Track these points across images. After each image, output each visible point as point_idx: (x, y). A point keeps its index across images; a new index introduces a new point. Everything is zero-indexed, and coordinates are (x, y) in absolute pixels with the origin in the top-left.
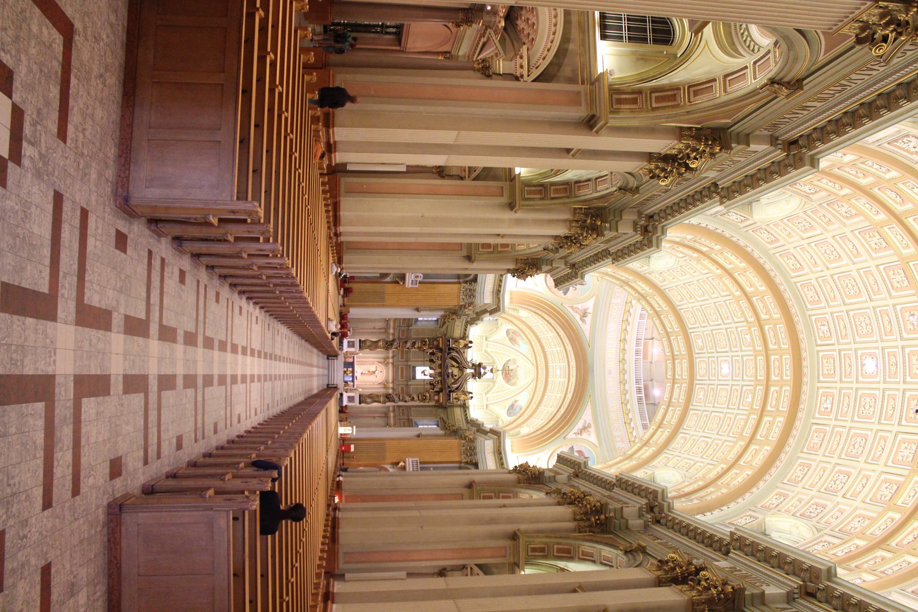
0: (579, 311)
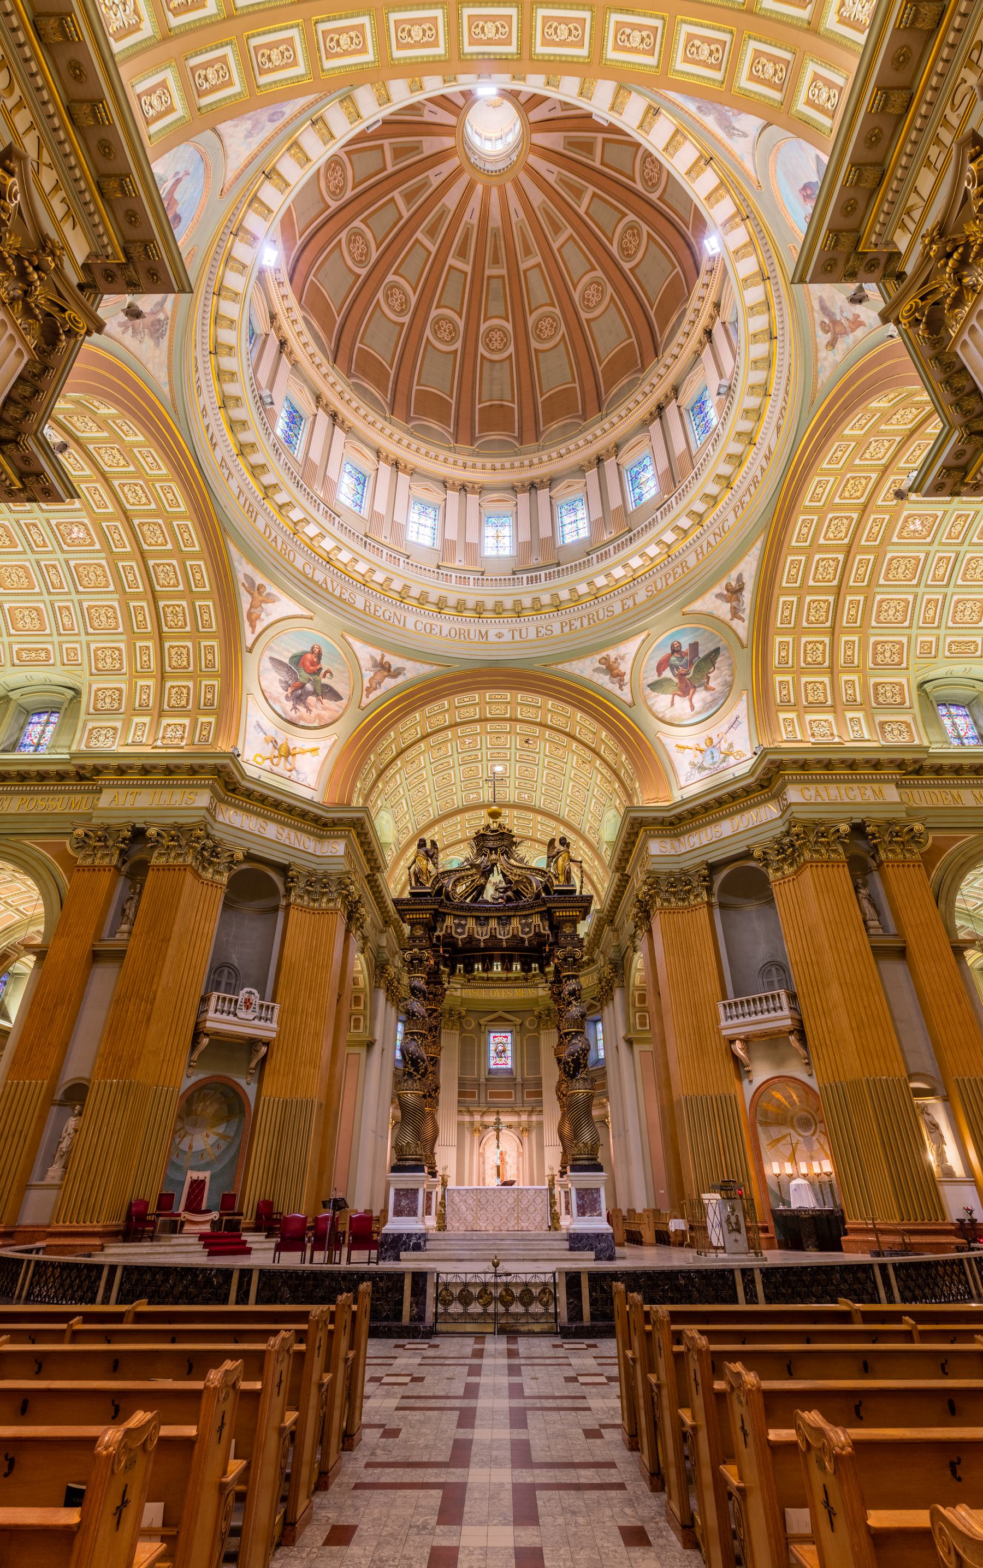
0: (378, 677)
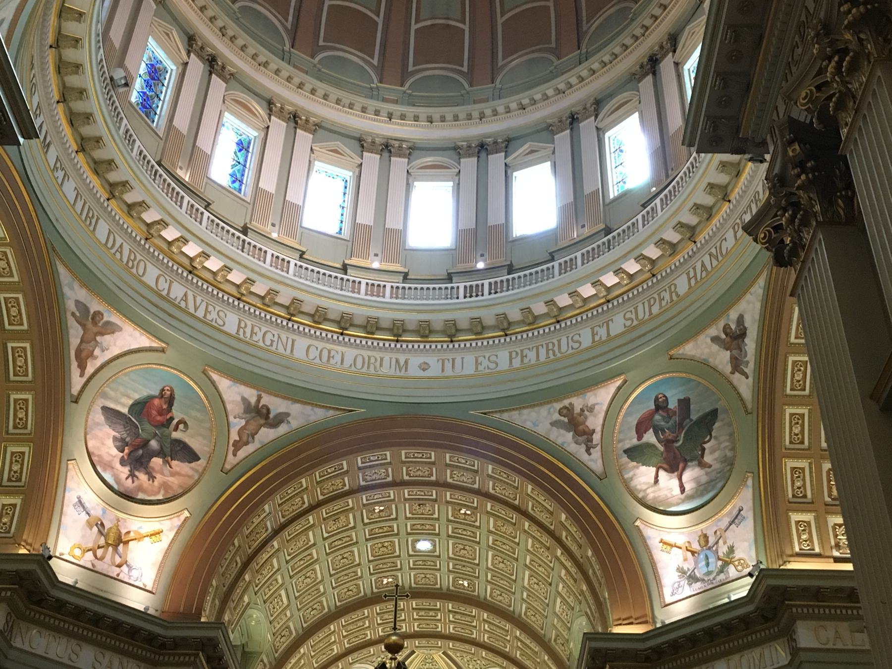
0: (251, 427)
